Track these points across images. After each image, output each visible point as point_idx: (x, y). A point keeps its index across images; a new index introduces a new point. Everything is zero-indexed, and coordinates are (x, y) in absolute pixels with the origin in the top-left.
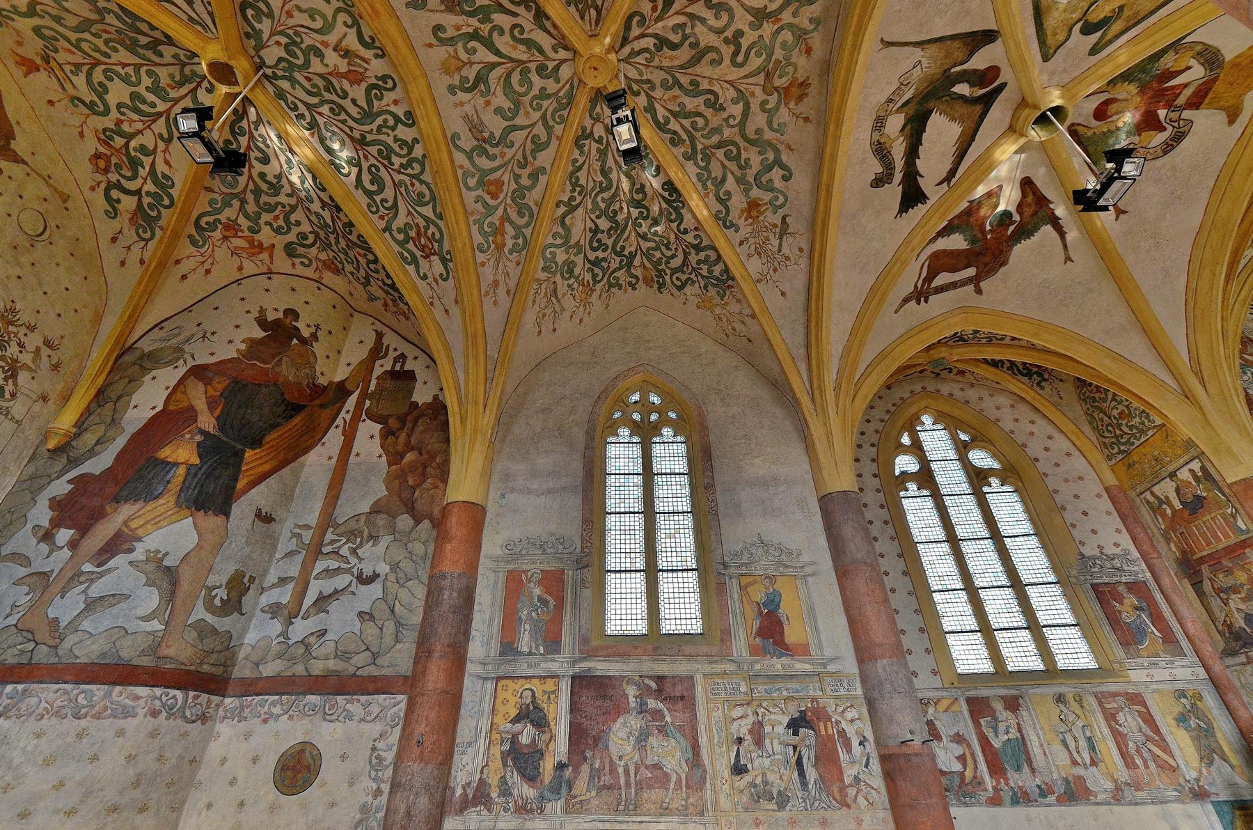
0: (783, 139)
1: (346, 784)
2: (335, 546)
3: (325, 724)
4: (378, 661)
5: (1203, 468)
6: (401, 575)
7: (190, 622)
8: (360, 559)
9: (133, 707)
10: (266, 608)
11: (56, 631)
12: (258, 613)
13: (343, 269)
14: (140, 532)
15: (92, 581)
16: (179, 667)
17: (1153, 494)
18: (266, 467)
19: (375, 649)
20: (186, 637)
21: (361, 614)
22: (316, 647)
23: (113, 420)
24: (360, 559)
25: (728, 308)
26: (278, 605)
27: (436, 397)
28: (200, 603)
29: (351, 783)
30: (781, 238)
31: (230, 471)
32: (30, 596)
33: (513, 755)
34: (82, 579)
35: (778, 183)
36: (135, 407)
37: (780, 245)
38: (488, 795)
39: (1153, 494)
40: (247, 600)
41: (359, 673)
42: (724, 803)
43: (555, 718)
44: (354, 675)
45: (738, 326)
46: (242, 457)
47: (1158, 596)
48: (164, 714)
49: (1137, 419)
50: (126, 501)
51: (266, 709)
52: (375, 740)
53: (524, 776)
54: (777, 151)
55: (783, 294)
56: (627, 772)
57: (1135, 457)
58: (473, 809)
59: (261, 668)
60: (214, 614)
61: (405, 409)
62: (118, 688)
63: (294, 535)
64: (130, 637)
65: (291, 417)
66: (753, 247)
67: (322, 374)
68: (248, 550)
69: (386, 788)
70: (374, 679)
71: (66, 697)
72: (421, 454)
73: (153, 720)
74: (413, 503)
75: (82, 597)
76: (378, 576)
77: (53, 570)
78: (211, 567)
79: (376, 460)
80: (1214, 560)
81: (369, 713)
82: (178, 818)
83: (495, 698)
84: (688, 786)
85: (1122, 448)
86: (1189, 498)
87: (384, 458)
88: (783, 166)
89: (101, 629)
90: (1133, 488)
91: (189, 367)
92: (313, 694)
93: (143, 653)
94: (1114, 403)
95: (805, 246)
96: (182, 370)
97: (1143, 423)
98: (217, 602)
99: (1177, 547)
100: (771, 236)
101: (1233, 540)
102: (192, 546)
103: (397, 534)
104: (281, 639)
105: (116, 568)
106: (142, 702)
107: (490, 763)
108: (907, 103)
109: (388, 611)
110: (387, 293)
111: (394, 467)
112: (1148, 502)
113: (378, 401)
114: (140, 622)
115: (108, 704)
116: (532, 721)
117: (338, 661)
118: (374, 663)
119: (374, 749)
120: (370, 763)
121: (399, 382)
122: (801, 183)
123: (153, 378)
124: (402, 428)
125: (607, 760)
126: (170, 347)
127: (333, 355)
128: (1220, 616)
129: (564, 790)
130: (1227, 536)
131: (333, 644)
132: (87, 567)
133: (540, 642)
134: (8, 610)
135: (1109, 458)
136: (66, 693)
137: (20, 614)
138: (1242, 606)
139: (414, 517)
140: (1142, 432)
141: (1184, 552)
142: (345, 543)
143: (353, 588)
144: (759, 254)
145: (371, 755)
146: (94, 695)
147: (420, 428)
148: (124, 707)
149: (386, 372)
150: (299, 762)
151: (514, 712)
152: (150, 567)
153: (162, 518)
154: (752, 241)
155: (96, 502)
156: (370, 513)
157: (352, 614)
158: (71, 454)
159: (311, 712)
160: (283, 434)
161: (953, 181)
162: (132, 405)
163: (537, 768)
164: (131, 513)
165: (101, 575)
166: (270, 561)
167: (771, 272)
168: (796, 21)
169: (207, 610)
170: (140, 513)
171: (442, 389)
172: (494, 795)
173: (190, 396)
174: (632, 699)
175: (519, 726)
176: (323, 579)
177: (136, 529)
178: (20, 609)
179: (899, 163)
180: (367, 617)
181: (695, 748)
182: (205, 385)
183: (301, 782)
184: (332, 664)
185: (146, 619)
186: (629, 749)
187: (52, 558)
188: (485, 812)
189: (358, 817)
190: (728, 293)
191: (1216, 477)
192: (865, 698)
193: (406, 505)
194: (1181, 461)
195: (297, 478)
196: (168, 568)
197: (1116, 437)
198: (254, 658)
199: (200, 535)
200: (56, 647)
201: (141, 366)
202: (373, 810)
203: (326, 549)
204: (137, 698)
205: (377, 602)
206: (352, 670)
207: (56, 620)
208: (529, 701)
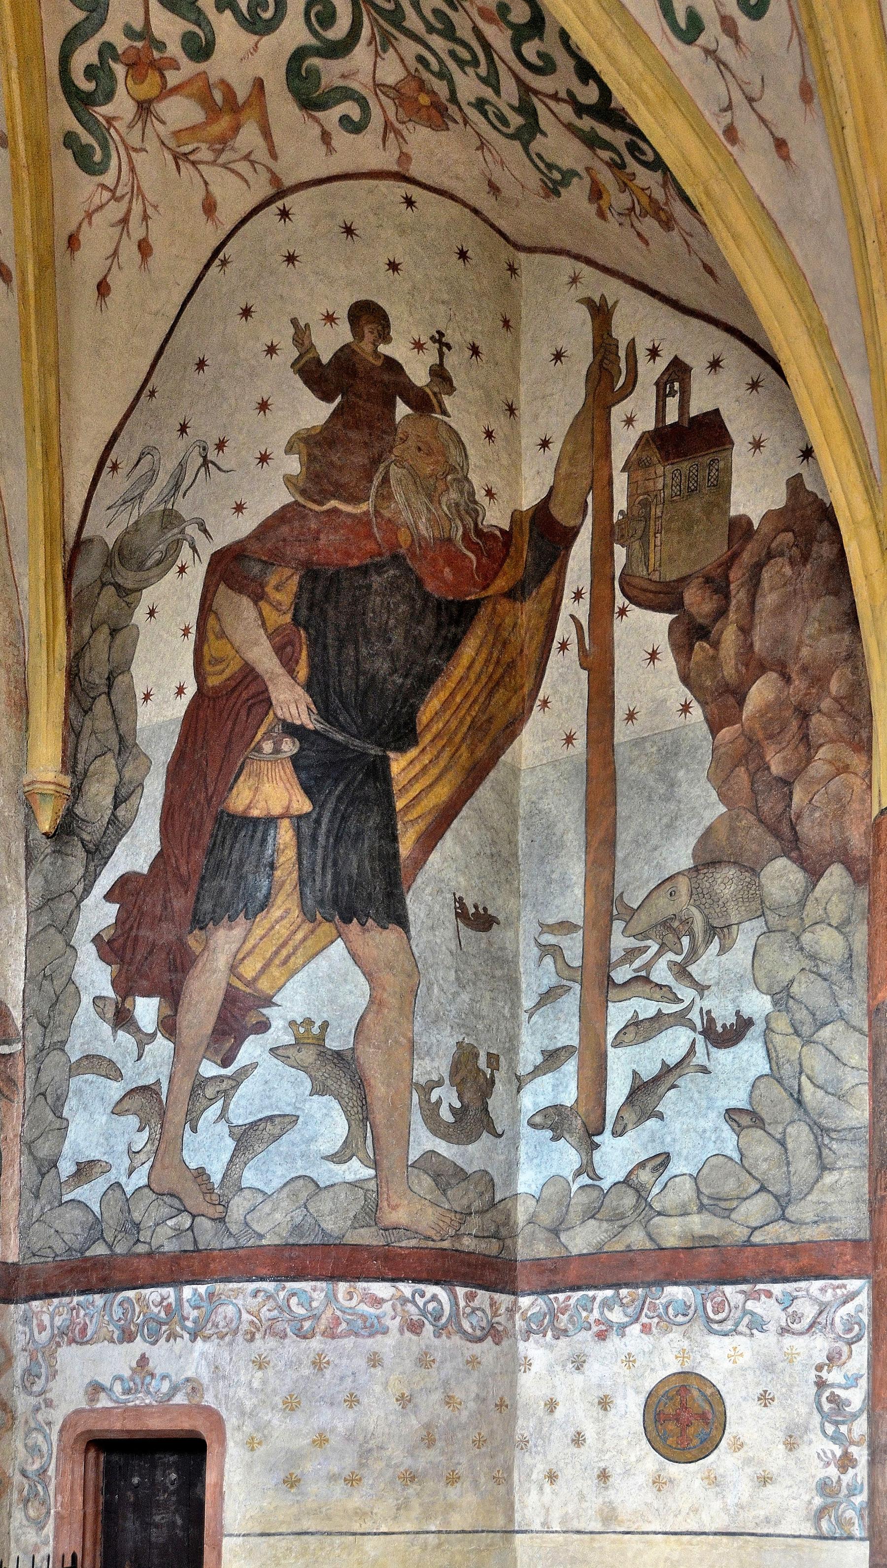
1: (781, 1447)
3: (713, 1339)
4: (792, 1212)
6: (802, 1015)
7: (412, 1158)
8: (701, 989)
9: (378, 1317)
10: (538, 1120)
11: (211, 1191)
12: (525, 1130)
13: (453, 98)
14: (264, 985)
15: (227, 1095)
16: (423, 1244)
18: (442, 793)
19: (779, 1188)
20: (416, 1188)
21: (731, 1114)
22: (656, 1190)
23: (121, 739)
24: (701, 989)
26: (558, 1109)
27: (795, 485)
28: (416, 1118)
29: (791, 1445)
31: (374, 820)
32: (145, 1134)
34: (210, 1092)
36: (147, 697)
40: (497, 1103)
41: (757, 1238)
44: (748, 1243)
46: (386, 779)
48: (429, 1328)
50: (216, 923)
51: (596, 1314)
52: (819, 1368)
59: (563, 1237)
60: (446, 1137)
61: (719, 549)
62: (342, 1287)
63: (547, 950)
64: (324, 1195)
65: (455, 644)
67: (489, 493)
68: (465, 997)
70: (793, 1250)
71: (271, 1304)
72: (788, 680)
73: (414, 1338)
75: (222, 1128)
76: (749, 1023)
77: (158, 1082)
78: (412, 1043)
79: (679, 720)
81: (796, 1317)
82: (510, 1492)
87: (697, 712)
89: (277, 1183)
91: (206, 560)
92: (675, 1284)
93: (357, 1223)
96: (198, 572)
98: (446, 1115)
102: (364, 1002)
104: (584, 1180)
105: (255, 1065)
106: (387, 1307)
109: (789, 1103)
110: (592, 141)
111: (726, 733)
113: (644, 539)
114: (332, 1166)
115: (338, 1313)
117: (706, 1216)
118: (783, 1218)
121: (685, 466)
123: (152, 613)
124: (721, 613)
126: (151, 515)
127: (499, 424)
131: (689, 1184)
132: (209, 1069)
134: (127, 1162)
136: (269, 1297)
137: (147, 1166)
139: (801, 862)
143: (700, 1058)
146: (312, 1300)
147: (769, 600)
148: (364, 1317)
149: (647, 440)
150: (684, 1407)
152: (308, 1055)
153: (289, 949)
155: (167, 933)
157: (712, 1115)
158: (87, 837)
159: (680, 1319)
160: (452, 694)
162: (140, 696)
164: (234, 947)
165: (237, 1080)
169: (435, 1132)
170: (249, 945)
171: (808, 453)
173: (237, 639)
177: (255, 979)
178: (142, 1157)
180: (745, 1120)
182: (256, 603)
183: (696, 1442)
184: (697, 1223)
185: (338, 1157)
187: (147, 1059)
195: (510, 803)
196: (338, 1054)
198: (546, 1219)
199: (369, 976)
200: (222, 1220)
201: (118, 586)
203: (621, 974)
204: (377, 1302)
205: (761, 1085)
206: (741, 1233)
207: (201, 1173)
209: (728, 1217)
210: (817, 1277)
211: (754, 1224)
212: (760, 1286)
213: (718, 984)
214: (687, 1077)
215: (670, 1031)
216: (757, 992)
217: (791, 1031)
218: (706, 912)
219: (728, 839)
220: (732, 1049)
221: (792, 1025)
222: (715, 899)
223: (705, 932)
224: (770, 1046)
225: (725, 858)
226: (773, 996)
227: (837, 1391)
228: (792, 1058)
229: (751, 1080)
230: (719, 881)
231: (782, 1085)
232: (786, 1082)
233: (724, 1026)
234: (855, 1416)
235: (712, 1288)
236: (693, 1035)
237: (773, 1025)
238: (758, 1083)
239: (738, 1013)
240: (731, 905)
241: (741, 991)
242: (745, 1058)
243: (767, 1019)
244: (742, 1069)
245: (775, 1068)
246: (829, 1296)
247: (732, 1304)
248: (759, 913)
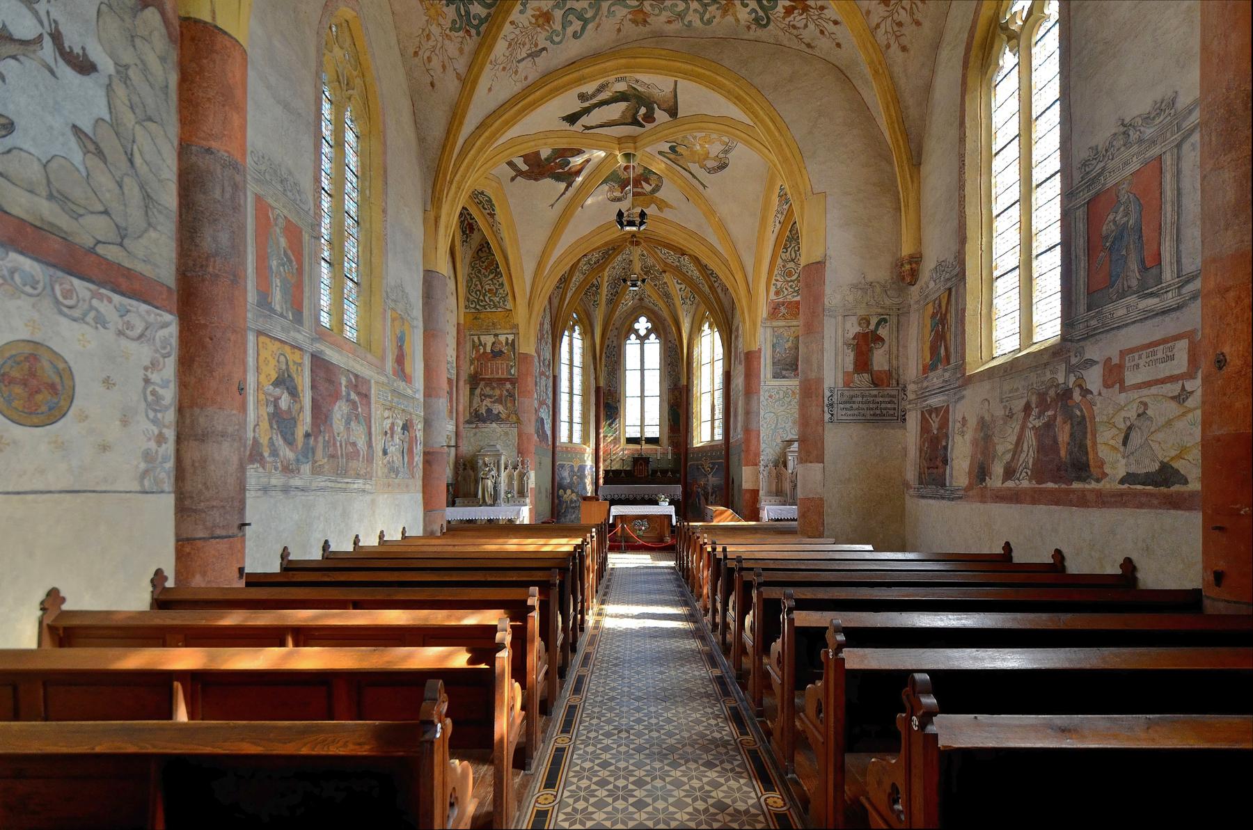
0: (604, 18)
1: (118, 423)
5: (513, 340)
17: (479, 338)
25: (447, 42)
29: (125, 422)
30: (529, 56)
33: (276, 419)
35: (570, 30)
37: (523, 59)
38: (261, 455)
39: (479, 338)
41: (100, 250)
42: (380, 473)
43: (302, 391)
44: (92, 251)
45: (436, 63)
47: (455, 389)
49: (498, 299)
52: (146, 369)
53: (285, 440)
54: (594, 17)
55: (490, 90)
56: (341, 445)
57: (482, 316)
58: (251, 466)
66: (513, 36)
69: (170, 434)
80: (489, 382)
81: (129, 326)
83: (258, 355)
84: (367, 461)
85: (478, 307)
86: (497, 350)
88: (583, 28)
90: (470, 329)
92: (22, 253)
94: (490, 282)
95: (531, 79)
97: (499, 302)
99: (474, 368)
100: (527, 46)
101: (505, 376)
107: (260, 423)
108: (635, 89)
112: (473, 341)
116: (288, 389)
118: (121, 245)
119: (147, 381)
120: (146, 400)
122: (573, 49)
125: (332, 435)
128: (475, 405)
129: (310, 455)
130: (503, 374)
133: (289, 306)
135: (466, 307)
138: (489, 405)
140: (495, 306)
141: (476, 373)
144: (510, 45)
145: (145, 389)
150: (32, 374)
151: (274, 376)
154: (517, 31)
161: (586, 131)
163: (293, 434)
167: (501, 67)
168: (691, 11)
172: (266, 454)
174: (344, 389)
175: (278, 391)
179: (594, 101)
181: (370, 434)
183: (44, 408)
186: (342, 428)
188: (261, 470)
189: (143, 466)
190: (461, 33)
191: (516, 346)
192: (424, 418)
194: (506, 332)
197: (478, 299)
202: (160, 459)
208: (284, 367)
209: (76, 219)
210: (145, 302)
211: (100, 238)
212: (103, 291)
227: (157, 389)
234: (167, 408)
235: (60, 274)
246: (152, 318)
247: (80, 296)
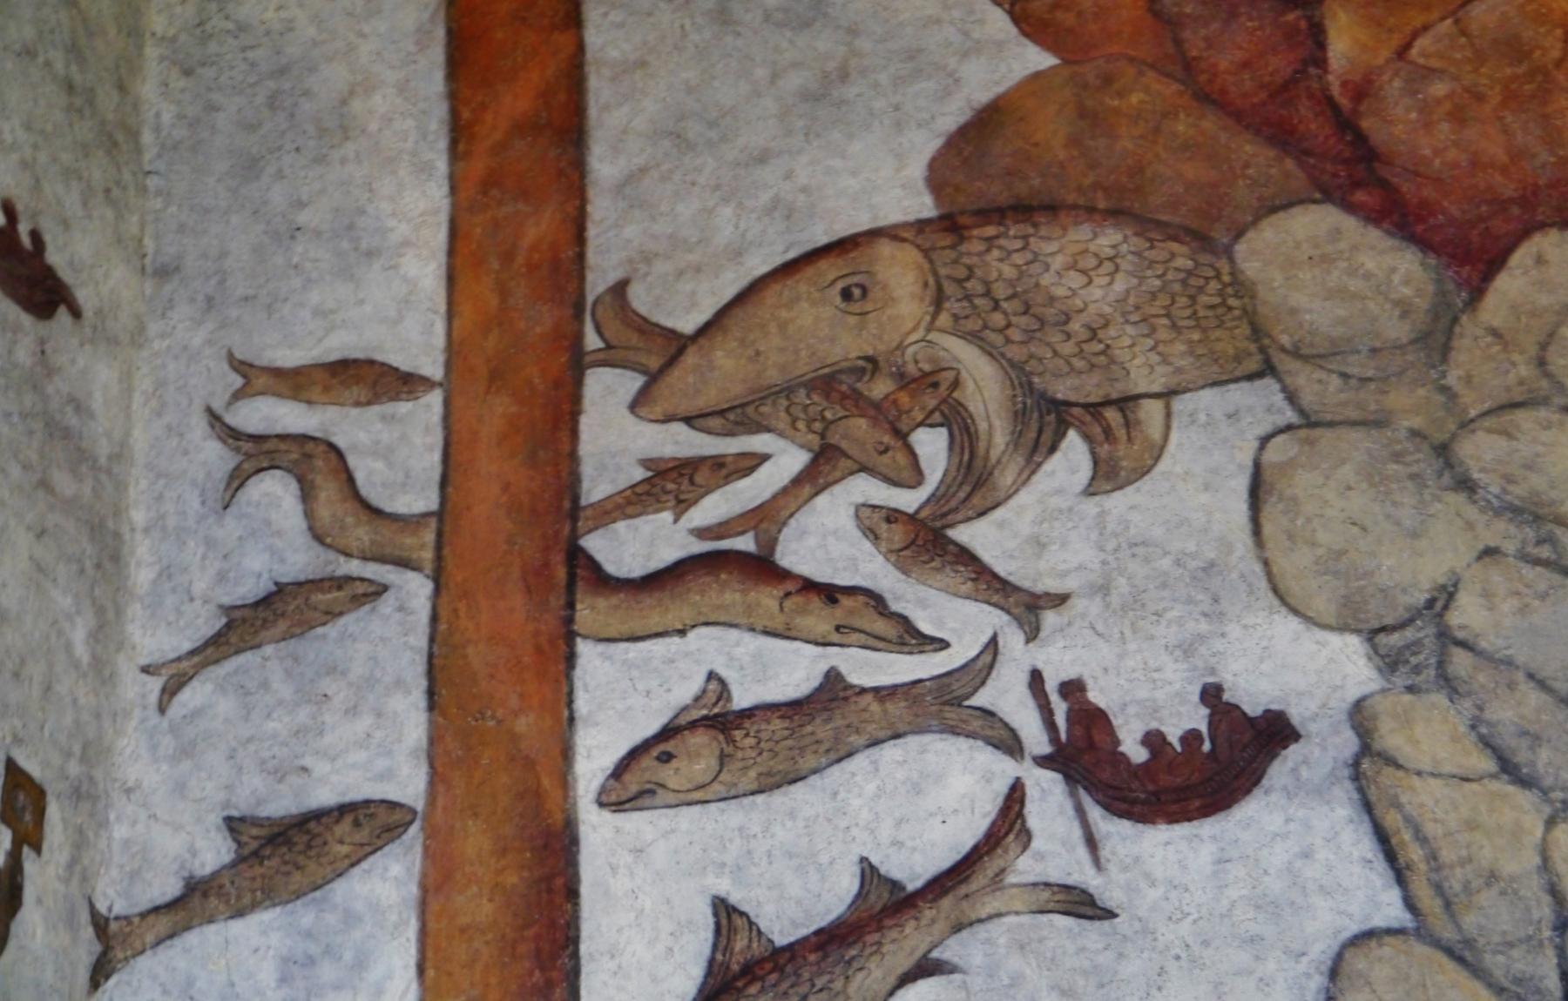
2: (714, 507)
74: (1346, 125)
103: (1305, 378)
142: (812, 480)
156: (950, 224)
166: (101, 672)
176: (698, 795)
193: (1282, 137)
213: (1103, 589)
214: (999, 931)
215: (891, 752)
216: (1286, 626)
217: (1487, 764)
218: (1015, 353)
219: (1074, 141)
220: (1208, 827)
221: (1487, 743)
222: (1050, 313)
223: (1019, 417)
224: (1392, 820)
225: (1071, 198)
226: (1372, 635)
228: (1509, 867)
229: (1322, 950)
230: (1058, 262)
231: (1477, 971)
232: (1495, 963)
233: (1154, 740)
236: (1005, 769)
237: (1390, 738)
238: (1357, 962)
239: (1212, 695)
240: (1123, 337)
241: (1216, 615)
242: (1278, 856)
243: (1360, 716)
244: (1267, 905)
245: (1428, 900)
248: (1253, 364)
